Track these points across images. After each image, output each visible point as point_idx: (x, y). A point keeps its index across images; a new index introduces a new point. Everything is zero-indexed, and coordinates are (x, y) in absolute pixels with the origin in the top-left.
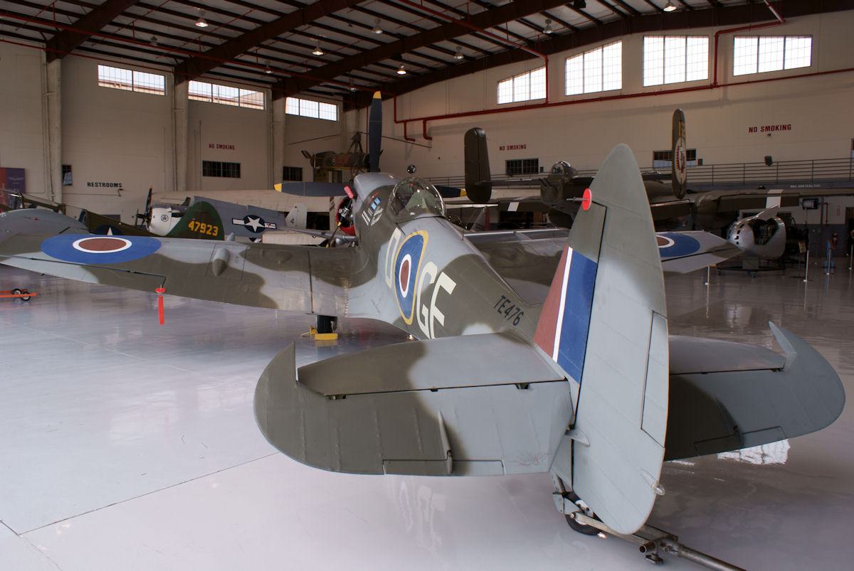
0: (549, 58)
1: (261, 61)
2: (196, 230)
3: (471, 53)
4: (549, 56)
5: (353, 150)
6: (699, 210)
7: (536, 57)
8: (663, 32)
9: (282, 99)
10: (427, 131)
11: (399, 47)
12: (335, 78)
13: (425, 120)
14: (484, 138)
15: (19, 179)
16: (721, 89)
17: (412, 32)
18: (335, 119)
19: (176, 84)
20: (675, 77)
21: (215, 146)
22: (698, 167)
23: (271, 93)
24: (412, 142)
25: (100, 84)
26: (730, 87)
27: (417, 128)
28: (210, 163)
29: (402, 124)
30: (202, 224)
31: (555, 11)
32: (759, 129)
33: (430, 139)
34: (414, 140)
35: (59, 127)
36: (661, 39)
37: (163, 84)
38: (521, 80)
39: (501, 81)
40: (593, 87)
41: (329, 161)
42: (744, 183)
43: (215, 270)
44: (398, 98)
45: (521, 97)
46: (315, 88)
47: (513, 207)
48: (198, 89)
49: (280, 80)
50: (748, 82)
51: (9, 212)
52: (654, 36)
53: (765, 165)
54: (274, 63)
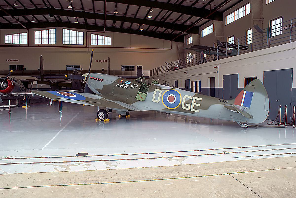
7: (23, 28)
20: (73, 43)
38: (16, 36)
40: (45, 42)
45: (16, 42)
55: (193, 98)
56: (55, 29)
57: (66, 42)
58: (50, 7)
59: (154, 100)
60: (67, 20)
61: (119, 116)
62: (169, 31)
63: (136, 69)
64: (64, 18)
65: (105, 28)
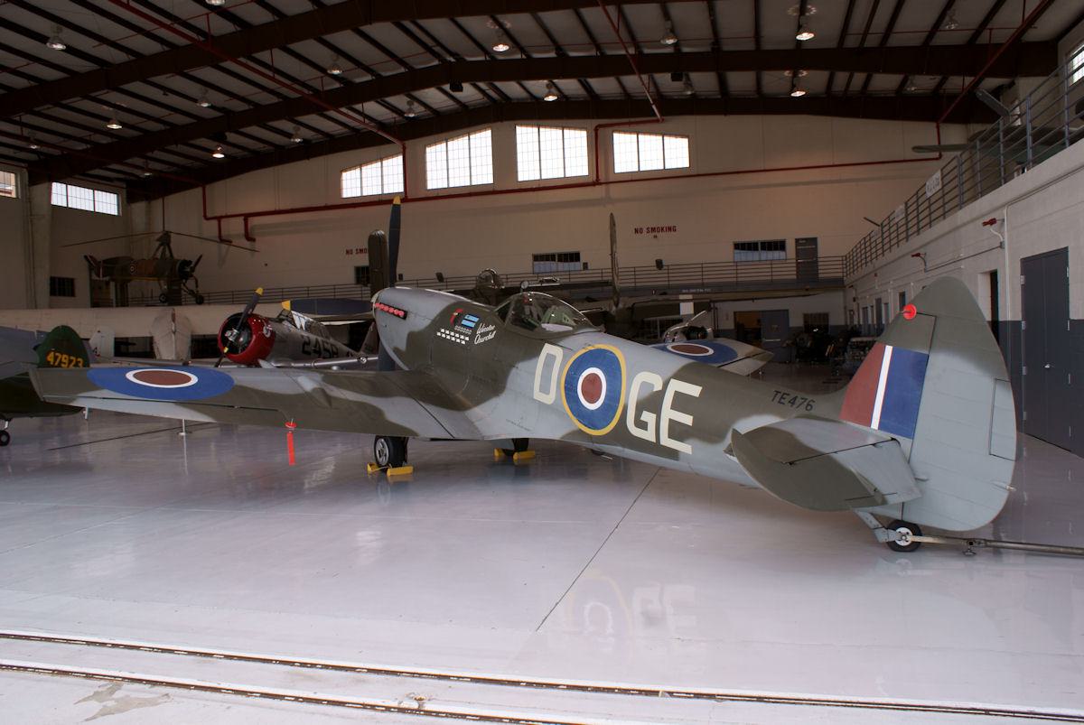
0: (406, 146)
1: (26, 132)
3: (309, 134)
4: (406, 142)
5: (159, 255)
6: (617, 319)
7: (389, 142)
8: (540, 122)
9: (46, 185)
10: (249, 231)
11: (220, 125)
13: (247, 216)
16: (604, 187)
17: (242, 107)
20: (552, 172)
22: (583, 272)
23: (27, 174)
26: (611, 185)
27: (236, 227)
30: (65, 356)
31: (419, 94)
32: (645, 230)
33: (254, 240)
36: (536, 129)
38: (371, 170)
39: (346, 170)
40: (460, 180)
42: (636, 289)
45: (372, 189)
49: (42, 157)
50: (632, 181)
52: (527, 125)
53: (655, 268)
54: (40, 135)
55: (666, 385)
56: (488, 133)
57: (527, 171)
58: (453, 60)
59: (538, 396)
60: (523, 94)
61: (496, 453)
62: (922, 83)
63: (791, 246)
64: (512, 89)
65: (654, 107)
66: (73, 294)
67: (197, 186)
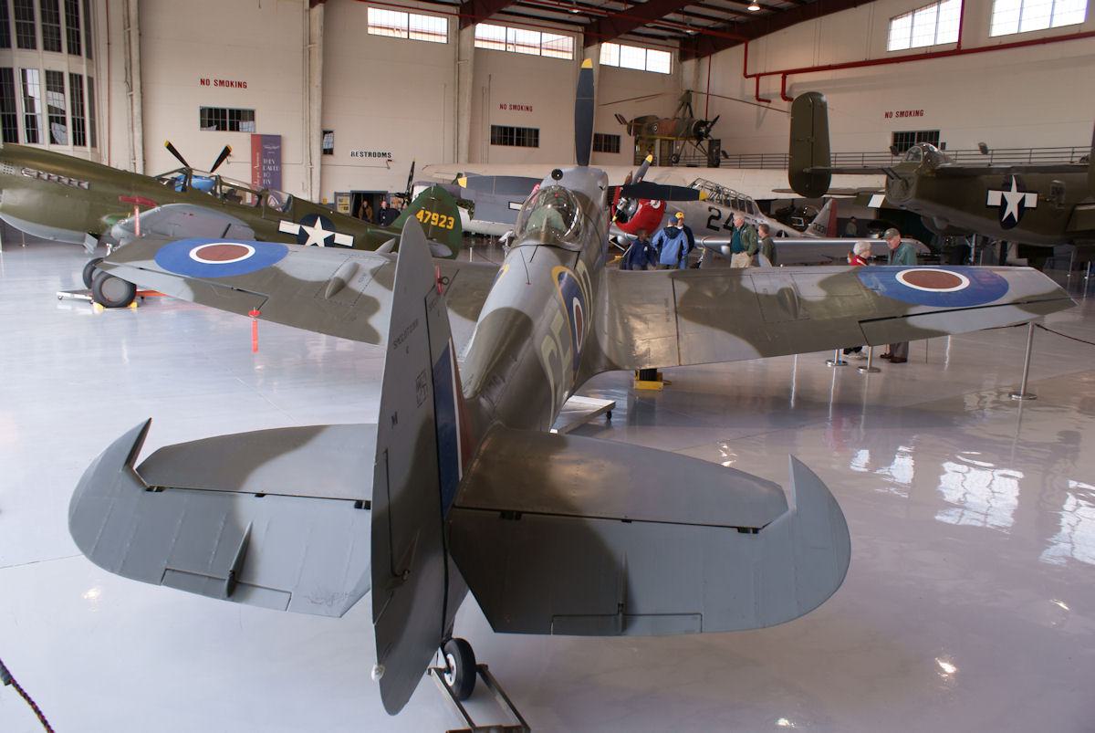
2: (425, 221)
5: (680, 115)
9: (596, 46)
10: (787, 90)
12: (665, 17)
13: (785, 74)
14: (823, 106)
15: (274, 148)
18: (668, 72)
19: (460, 29)
21: (508, 107)
23: (582, 36)
24: (765, 104)
25: (371, 31)
27: (772, 85)
28: (500, 128)
29: (754, 80)
30: (434, 214)
34: (769, 101)
35: (320, 85)
37: (446, 29)
38: (925, 16)
41: (650, 128)
43: (328, 291)
44: (751, 44)
45: (923, 40)
46: (640, 30)
47: (877, 201)
48: (488, 34)
51: (164, 206)
66: (618, 151)
67: (737, 43)
